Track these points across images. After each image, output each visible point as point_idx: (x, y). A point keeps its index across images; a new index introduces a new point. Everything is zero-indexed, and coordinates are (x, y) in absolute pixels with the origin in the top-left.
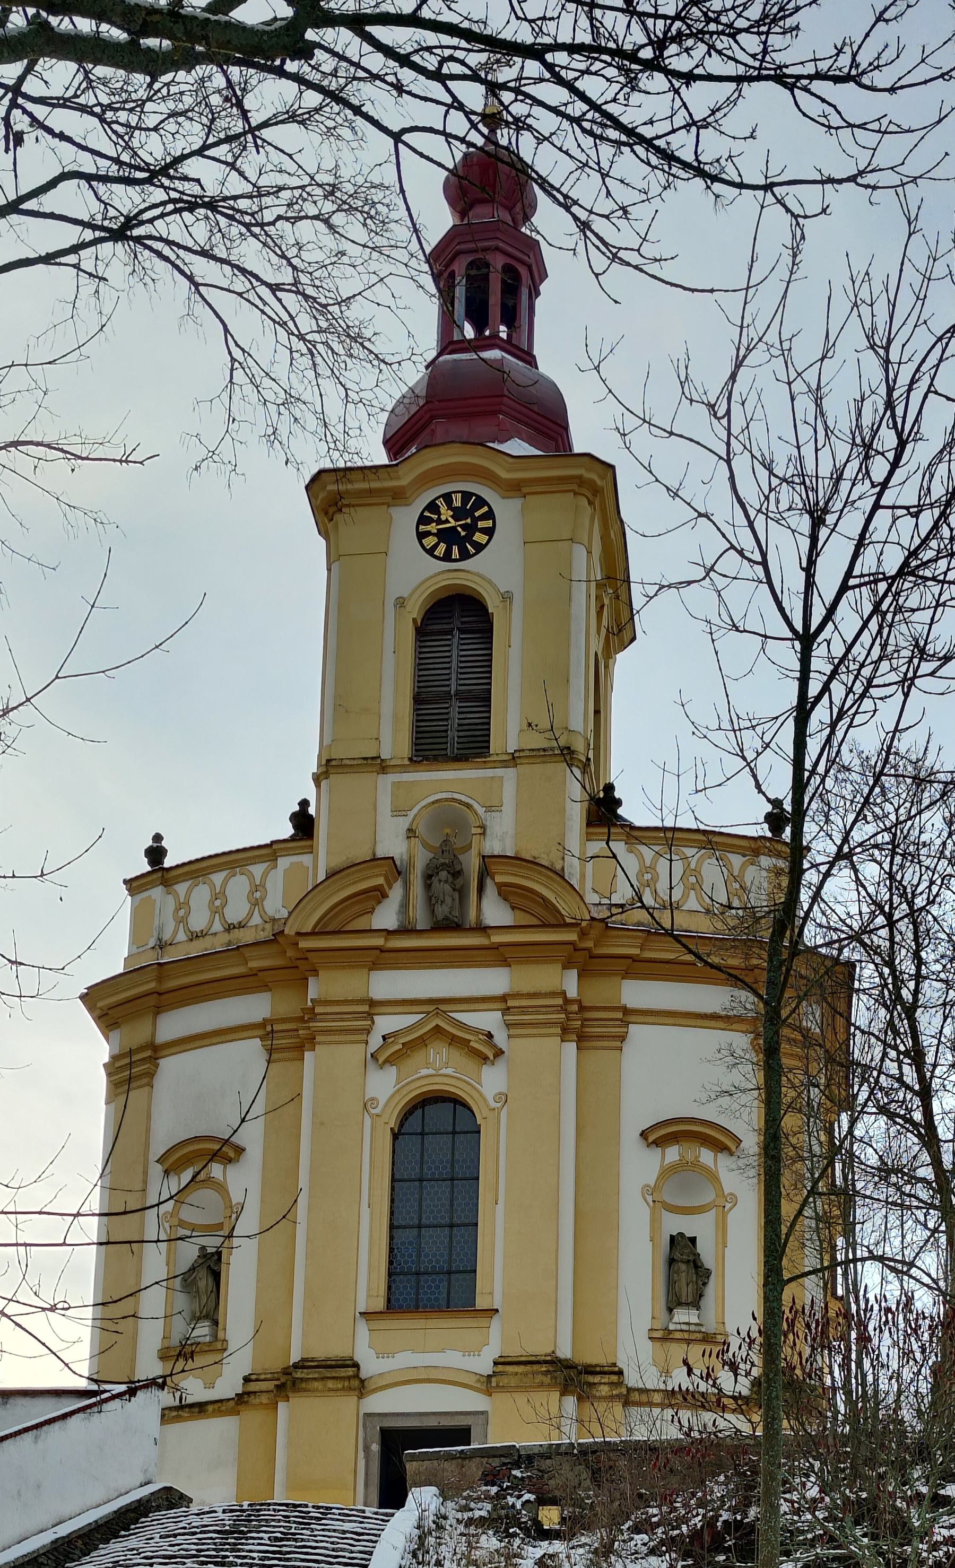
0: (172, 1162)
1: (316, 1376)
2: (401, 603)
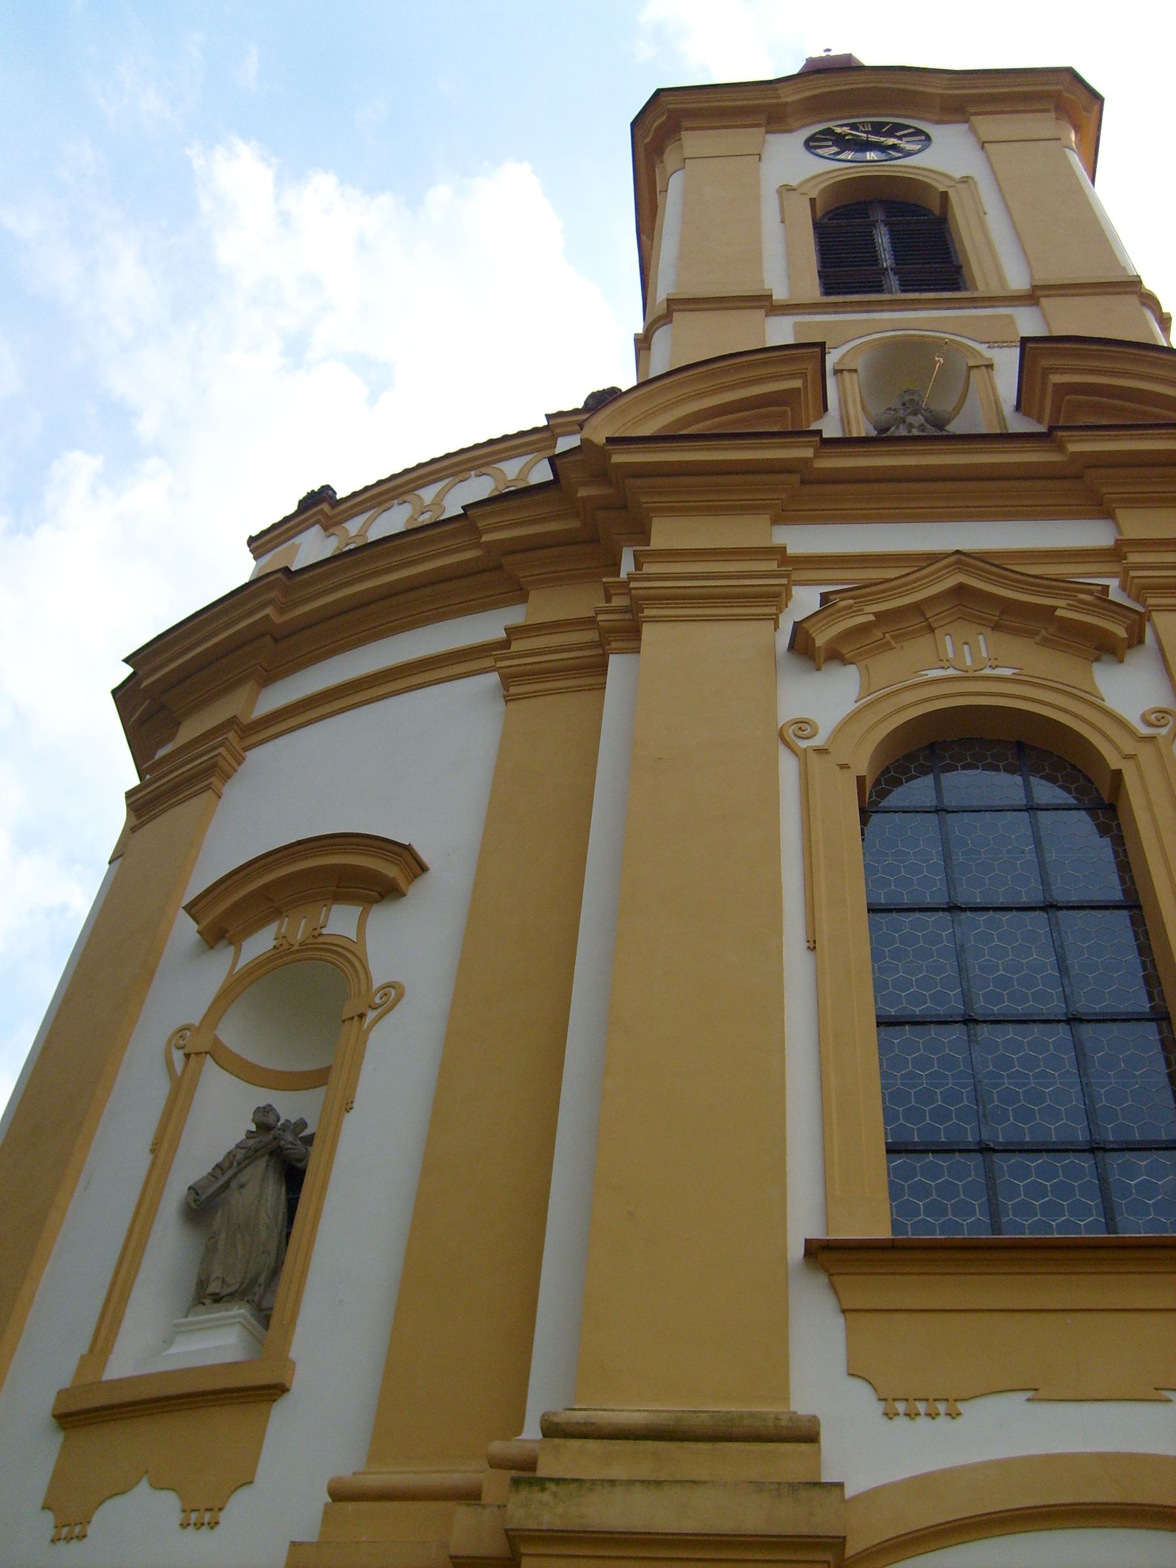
0: (230, 910)
1: (644, 1471)
2: (788, 189)
